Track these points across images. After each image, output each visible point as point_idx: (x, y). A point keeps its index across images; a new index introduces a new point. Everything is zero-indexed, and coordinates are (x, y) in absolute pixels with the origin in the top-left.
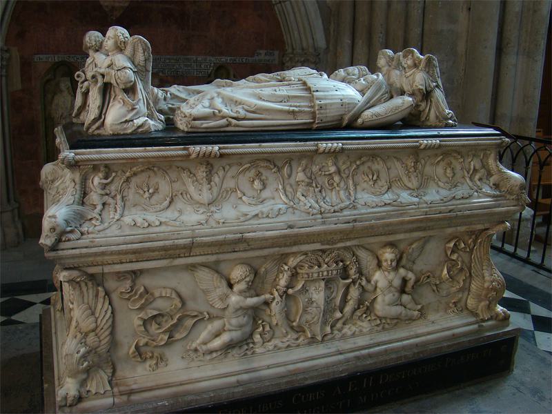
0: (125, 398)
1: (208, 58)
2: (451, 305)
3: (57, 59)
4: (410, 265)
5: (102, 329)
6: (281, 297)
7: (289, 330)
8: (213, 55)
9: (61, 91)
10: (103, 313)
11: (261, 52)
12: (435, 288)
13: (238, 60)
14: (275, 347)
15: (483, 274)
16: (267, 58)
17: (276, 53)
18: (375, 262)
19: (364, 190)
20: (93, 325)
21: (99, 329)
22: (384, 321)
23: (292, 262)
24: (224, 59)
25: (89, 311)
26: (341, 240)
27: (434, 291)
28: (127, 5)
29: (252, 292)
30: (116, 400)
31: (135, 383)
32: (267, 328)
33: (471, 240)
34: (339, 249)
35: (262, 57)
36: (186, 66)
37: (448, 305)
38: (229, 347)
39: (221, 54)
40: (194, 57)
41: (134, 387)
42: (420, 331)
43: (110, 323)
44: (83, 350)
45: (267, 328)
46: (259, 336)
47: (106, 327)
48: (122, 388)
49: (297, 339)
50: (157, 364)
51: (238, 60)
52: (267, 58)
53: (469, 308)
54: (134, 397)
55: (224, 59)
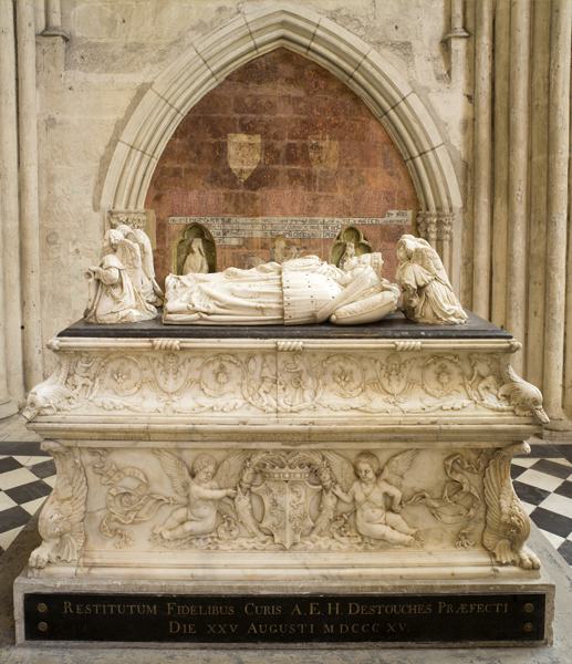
0: (86, 570)
1: (336, 219)
3: (190, 220)
4: (394, 479)
8: (340, 216)
9: (193, 252)
11: (392, 212)
13: (367, 221)
15: (499, 504)
16: (400, 218)
17: (410, 213)
20: (70, 494)
23: (256, 459)
24: (352, 221)
25: (67, 481)
26: (304, 442)
28: (255, 167)
29: (214, 484)
30: (79, 571)
31: (100, 558)
34: (304, 451)
35: (394, 217)
36: (312, 227)
39: (350, 215)
40: (321, 219)
41: (98, 561)
44: (56, 517)
48: (87, 560)
51: (367, 221)
52: (400, 218)
54: (94, 571)
55: (352, 221)
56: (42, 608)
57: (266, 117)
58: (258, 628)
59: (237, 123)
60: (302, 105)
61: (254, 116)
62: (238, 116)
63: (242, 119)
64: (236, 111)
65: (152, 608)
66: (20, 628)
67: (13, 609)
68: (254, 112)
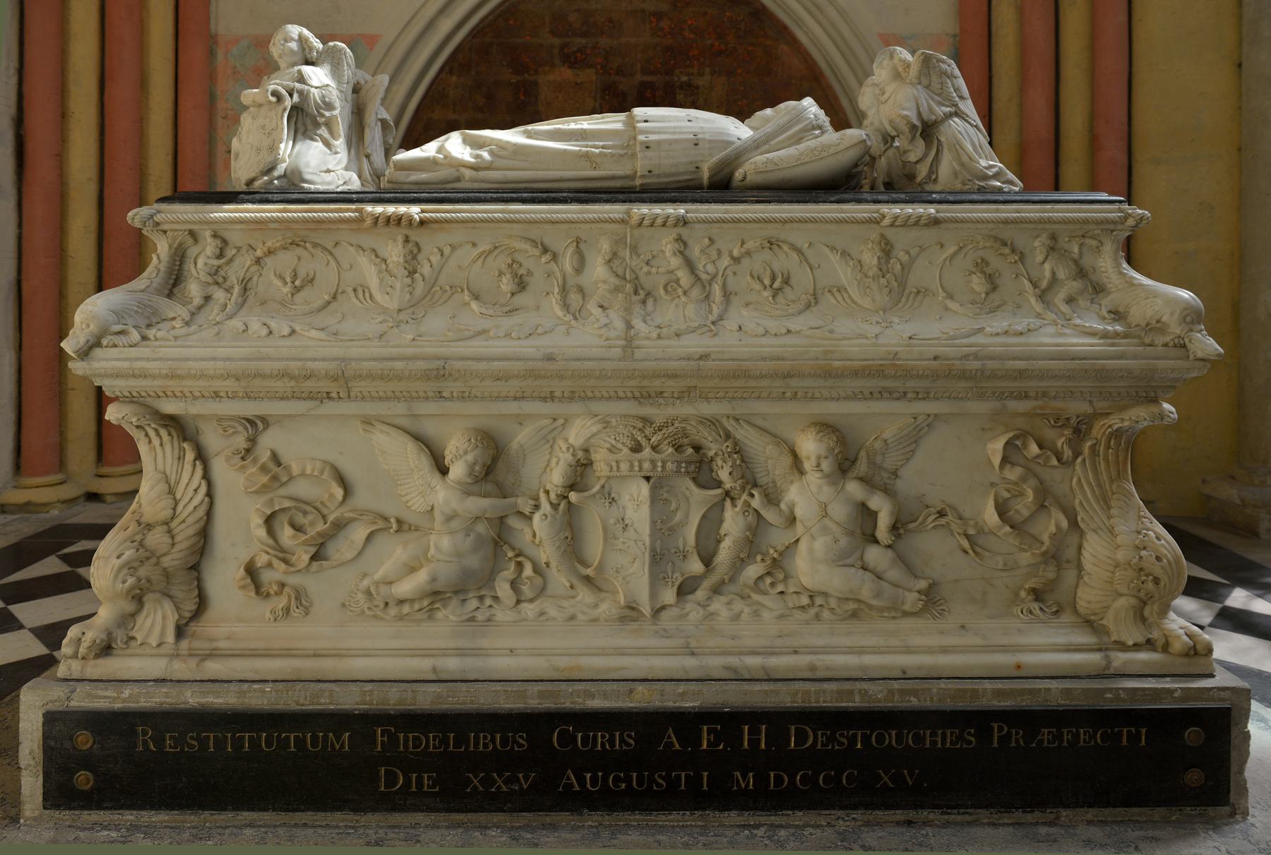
2: (1023, 594)
5: (184, 521)
6: (555, 507)
7: (576, 582)
10: (190, 493)
12: (966, 544)
14: (542, 614)
18: (788, 460)
19: (747, 305)
21: (176, 522)
22: (819, 601)
27: (966, 552)
32: (528, 571)
33: (1063, 439)
37: (1017, 594)
38: (435, 596)
42: (917, 641)
43: (201, 512)
45: (528, 571)
46: (507, 586)
47: (191, 520)
49: (596, 606)
50: (287, 610)
53: (1081, 610)
56: (84, 740)
57: (604, 42)
58: (581, 781)
59: (556, 51)
60: (665, 24)
61: (584, 41)
62: (556, 41)
63: (563, 47)
64: (553, 33)
65: (338, 738)
66: (31, 785)
67: (18, 744)
68: (584, 35)
